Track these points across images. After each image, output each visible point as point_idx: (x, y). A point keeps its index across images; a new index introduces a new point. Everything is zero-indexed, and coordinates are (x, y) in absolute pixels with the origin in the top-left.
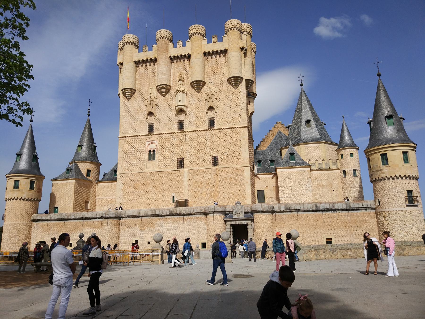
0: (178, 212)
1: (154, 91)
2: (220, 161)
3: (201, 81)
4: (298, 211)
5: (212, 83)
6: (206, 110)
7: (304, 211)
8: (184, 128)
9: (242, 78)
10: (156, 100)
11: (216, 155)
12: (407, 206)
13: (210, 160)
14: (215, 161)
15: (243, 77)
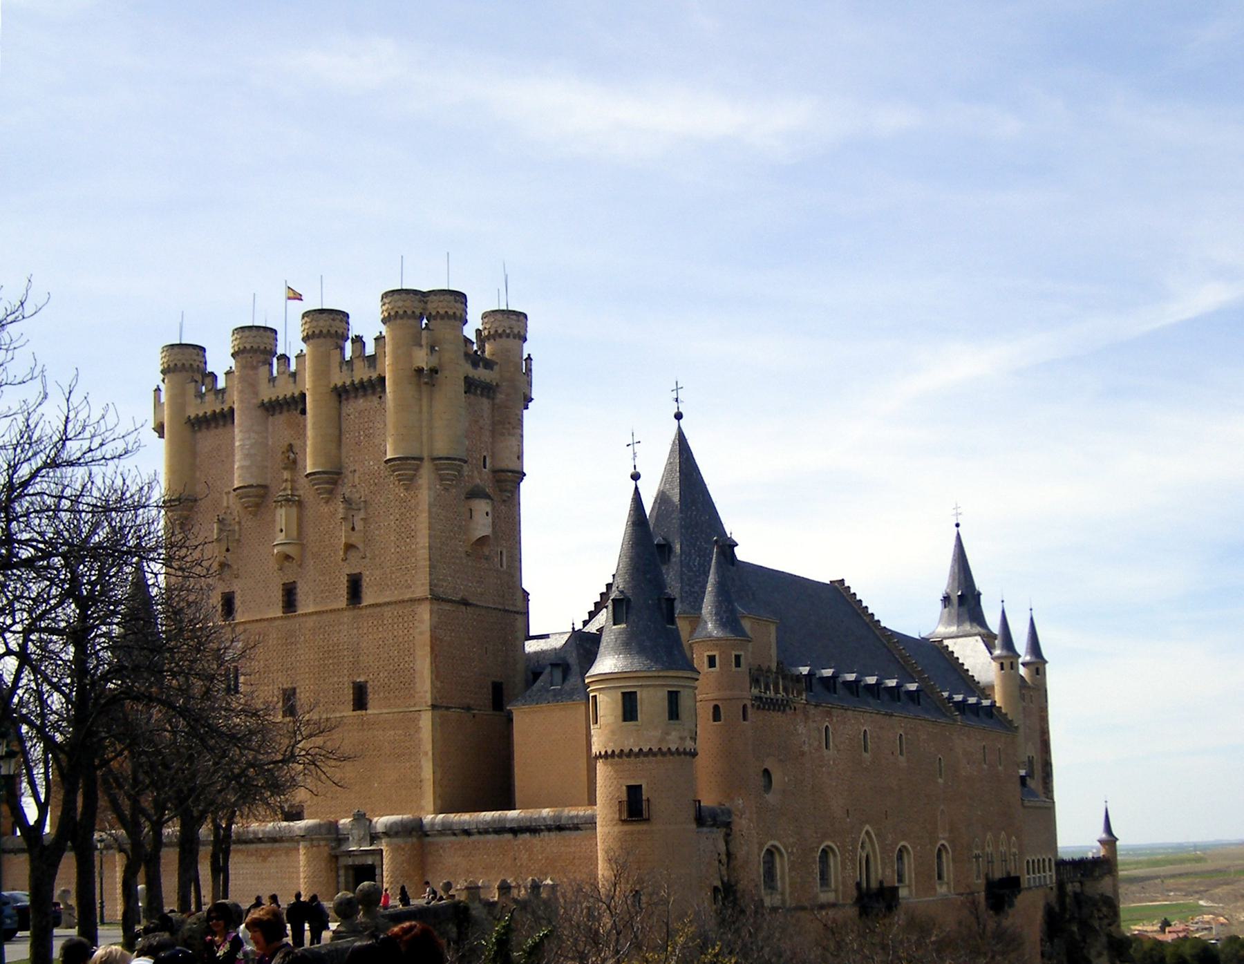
0: (251, 836)
1: (232, 503)
2: (371, 696)
3: (324, 473)
4: (467, 833)
5: (357, 475)
6: (341, 553)
7: (479, 833)
8: (298, 604)
9: (421, 459)
10: (237, 528)
11: (362, 679)
12: (624, 822)
13: (349, 695)
14: (360, 699)
15: (425, 455)
